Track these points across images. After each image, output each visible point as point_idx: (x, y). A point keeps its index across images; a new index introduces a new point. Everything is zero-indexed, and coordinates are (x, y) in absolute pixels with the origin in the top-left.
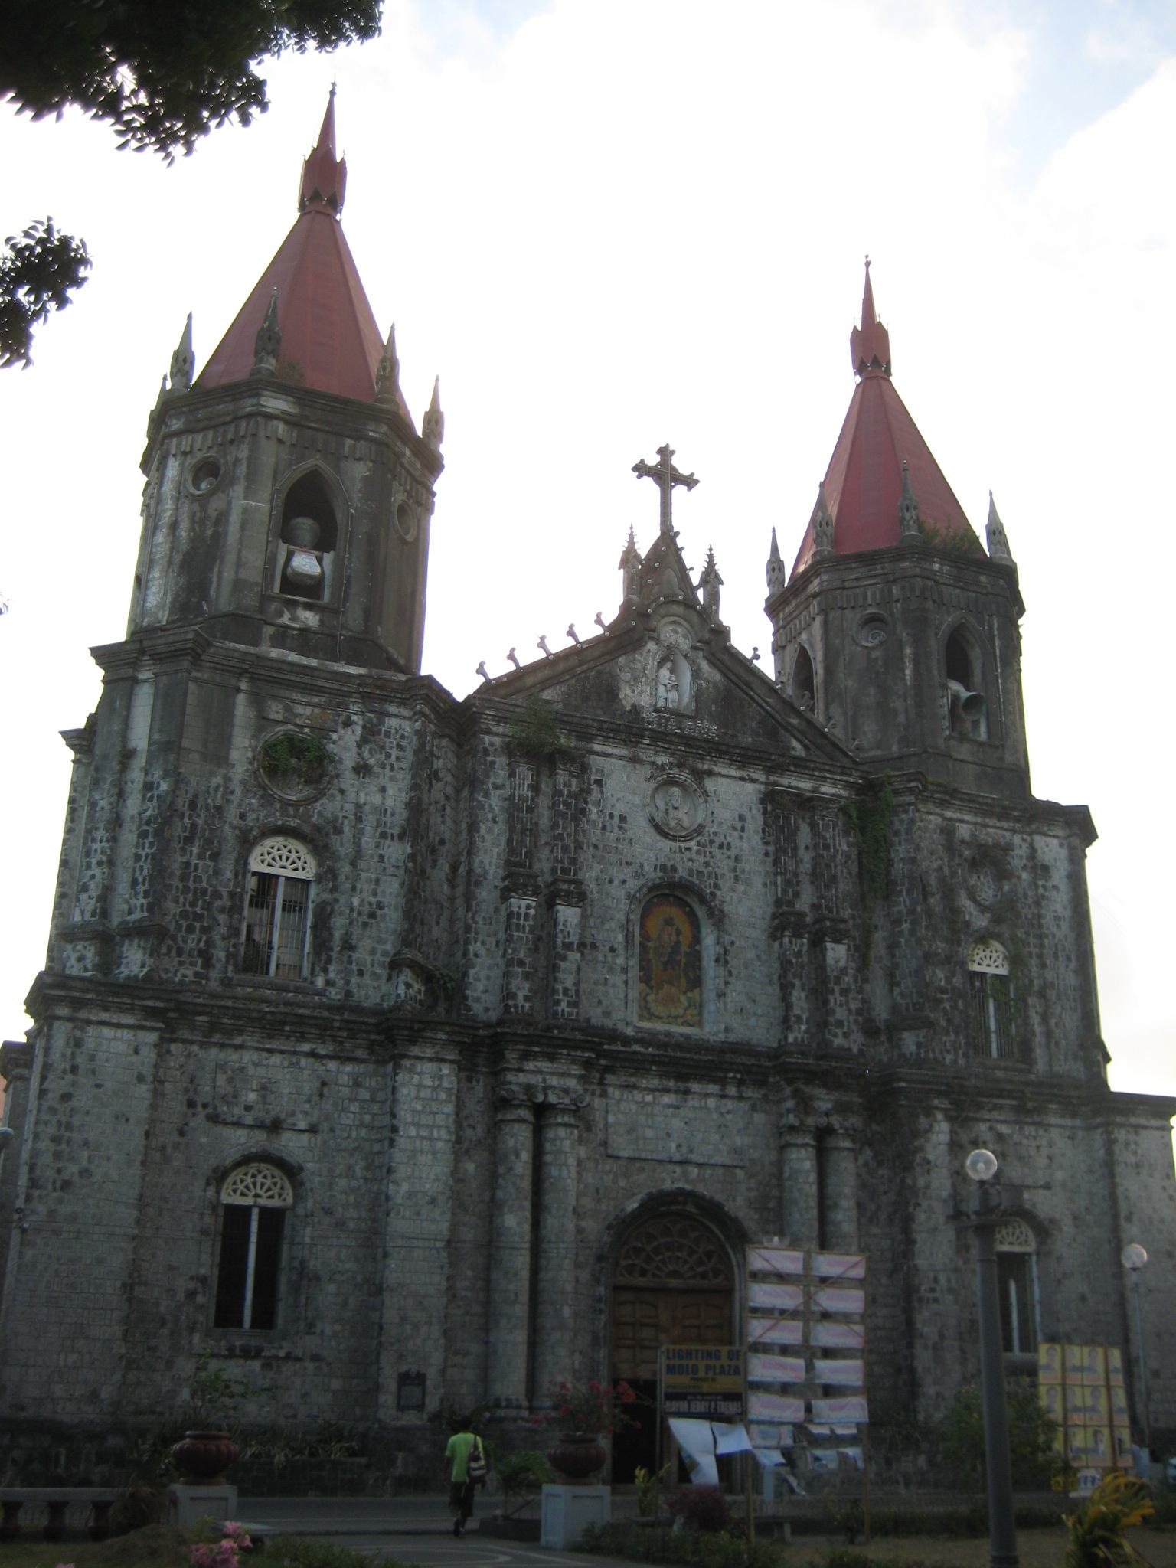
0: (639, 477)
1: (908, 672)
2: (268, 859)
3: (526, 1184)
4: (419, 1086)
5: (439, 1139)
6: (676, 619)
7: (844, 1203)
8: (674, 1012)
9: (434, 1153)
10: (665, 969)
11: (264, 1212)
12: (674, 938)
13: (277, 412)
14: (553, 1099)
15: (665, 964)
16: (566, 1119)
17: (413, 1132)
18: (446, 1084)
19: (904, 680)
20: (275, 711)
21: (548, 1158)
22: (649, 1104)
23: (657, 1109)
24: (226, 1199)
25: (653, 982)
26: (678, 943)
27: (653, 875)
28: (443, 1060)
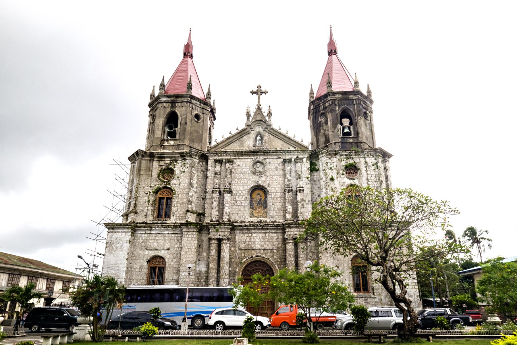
0: (252, 94)
1: (329, 124)
2: (162, 194)
3: (216, 257)
4: (188, 237)
5: (193, 249)
6: (259, 124)
7: (301, 256)
8: (260, 214)
9: (192, 252)
10: (258, 205)
11: (159, 267)
12: (260, 197)
14: (221, 237)
15: (257, 204)
16: (225, 242)
17: (186, 248)
18: (194, 236)
19: (328, 126)
20: (162, 163)
21: (221, 251)
23: (252, 237)
25: (254, 209)
26: (261, 199)
27: (253, 185)
28: (194, 231)
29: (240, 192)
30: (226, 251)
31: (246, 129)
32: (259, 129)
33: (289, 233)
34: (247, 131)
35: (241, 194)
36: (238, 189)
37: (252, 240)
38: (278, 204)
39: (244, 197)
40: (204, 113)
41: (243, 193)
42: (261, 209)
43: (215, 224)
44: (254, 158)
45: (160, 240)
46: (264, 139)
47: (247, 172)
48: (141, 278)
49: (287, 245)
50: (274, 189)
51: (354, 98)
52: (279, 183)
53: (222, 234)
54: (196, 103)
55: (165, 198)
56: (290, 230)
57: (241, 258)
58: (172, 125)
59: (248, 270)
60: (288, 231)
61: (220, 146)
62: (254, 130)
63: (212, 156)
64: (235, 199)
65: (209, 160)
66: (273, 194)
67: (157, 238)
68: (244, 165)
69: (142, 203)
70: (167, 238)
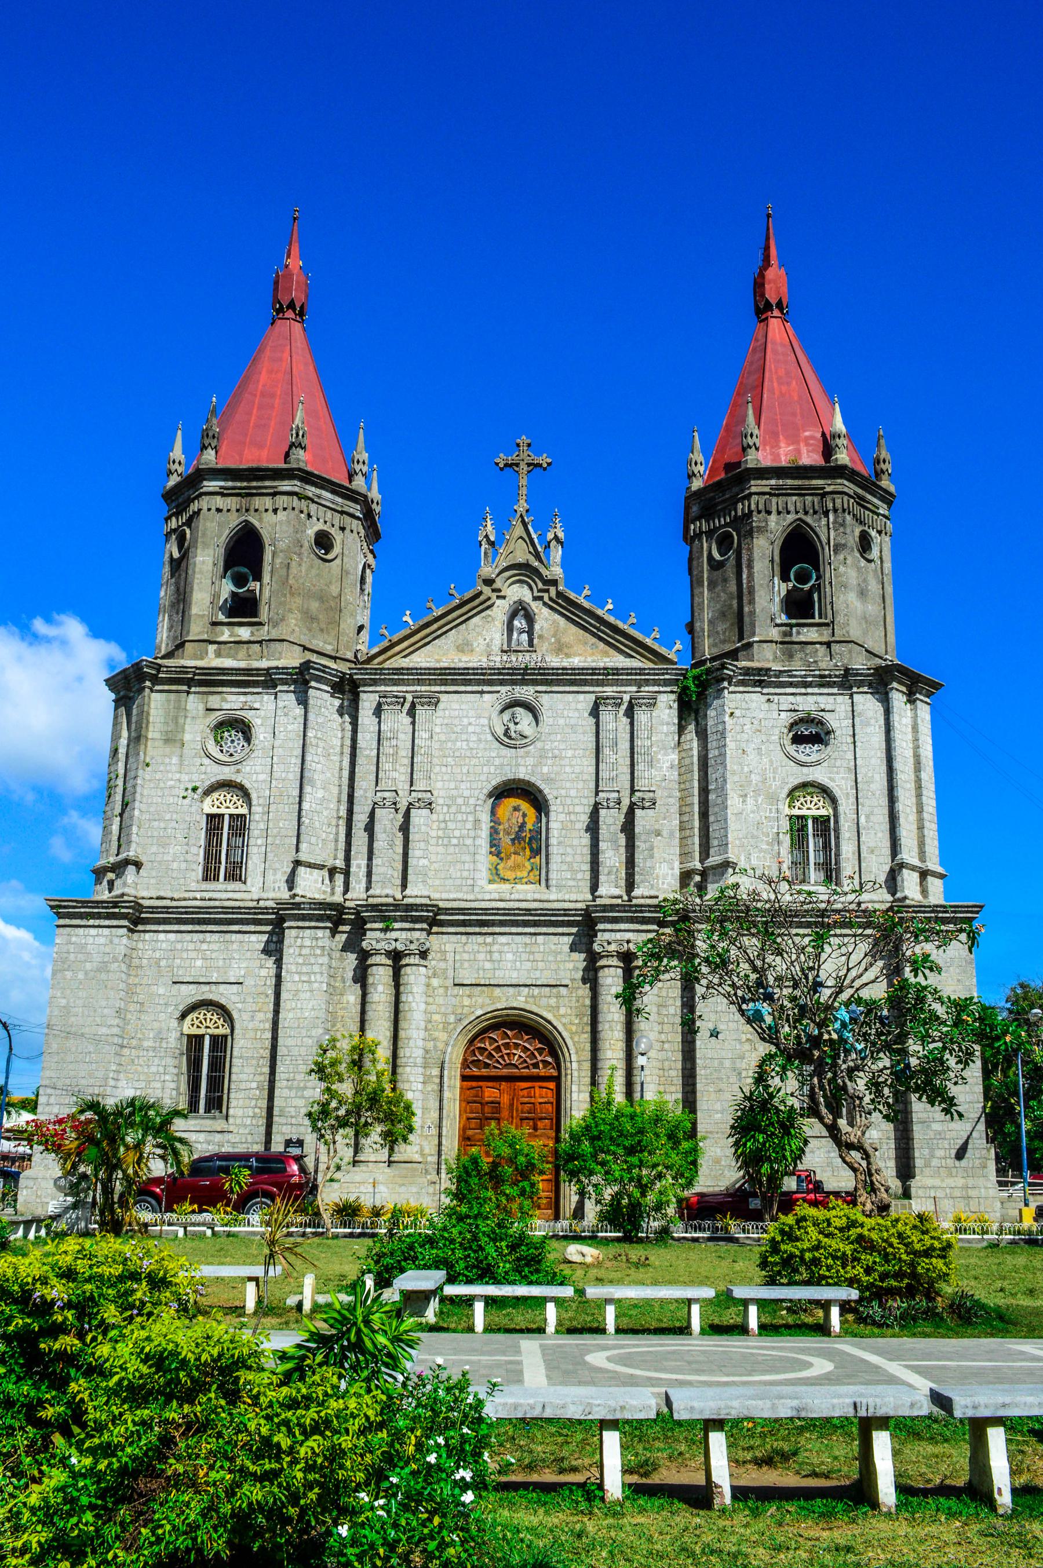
2: (217, 803)
4: (301, 947)
8: (519, 874)
10: (513, 844)
11: (214, 1038)
13: (217, 489)
14: (400, 947)
15: (513, 840)
17: (296, 978)
20: (214, 701)
22: (490, 944)
23: (495, 948)
24: (186, 1031)
29: (460, 801)
30: (415, 990)
31: (481, 593)
32: (519, 592)
33: (607, 936)
34: (482, 598)
35: (463, 809)
36: (454, 793)
37: (496, 956)
38: (576, 842)
39: (471, 818)
40: (343, 529)
41: (467, 804)
42: (523, 859)
43: (382, 905)
44: (503, 689)
45: (212, 951)
46: (537, 627)
47: (483, 737)
48: (161, 1069)
49: (601, 974)
50: (563, 792)
51: (828, 489)
52: (582, 773)
53: (403, 935)
54: (319, 497)
55: (227, 818)
56: (609, 926)
57: (459, 1011)
58: (246, 570)
59: (482, 1050)
60: (604, 931)
61: (397, 649)
62: (504, 597)
63: (375, 682)
64: (443, 825)
65: (363, 696)
66: (560, 809)
67: (205, 946)
68: (471, 713)
69: (155, 834)
70: (235, 946)
